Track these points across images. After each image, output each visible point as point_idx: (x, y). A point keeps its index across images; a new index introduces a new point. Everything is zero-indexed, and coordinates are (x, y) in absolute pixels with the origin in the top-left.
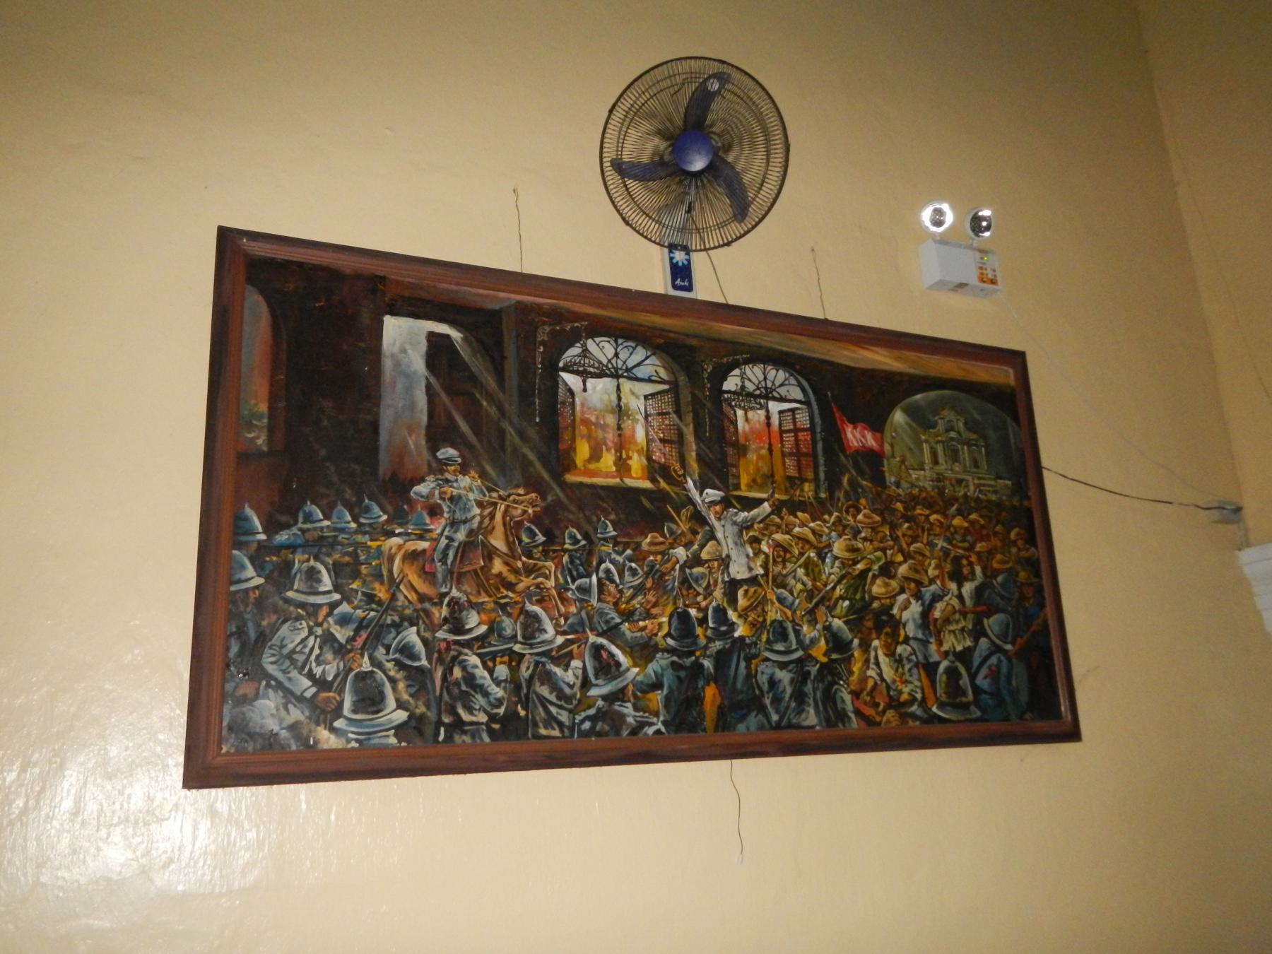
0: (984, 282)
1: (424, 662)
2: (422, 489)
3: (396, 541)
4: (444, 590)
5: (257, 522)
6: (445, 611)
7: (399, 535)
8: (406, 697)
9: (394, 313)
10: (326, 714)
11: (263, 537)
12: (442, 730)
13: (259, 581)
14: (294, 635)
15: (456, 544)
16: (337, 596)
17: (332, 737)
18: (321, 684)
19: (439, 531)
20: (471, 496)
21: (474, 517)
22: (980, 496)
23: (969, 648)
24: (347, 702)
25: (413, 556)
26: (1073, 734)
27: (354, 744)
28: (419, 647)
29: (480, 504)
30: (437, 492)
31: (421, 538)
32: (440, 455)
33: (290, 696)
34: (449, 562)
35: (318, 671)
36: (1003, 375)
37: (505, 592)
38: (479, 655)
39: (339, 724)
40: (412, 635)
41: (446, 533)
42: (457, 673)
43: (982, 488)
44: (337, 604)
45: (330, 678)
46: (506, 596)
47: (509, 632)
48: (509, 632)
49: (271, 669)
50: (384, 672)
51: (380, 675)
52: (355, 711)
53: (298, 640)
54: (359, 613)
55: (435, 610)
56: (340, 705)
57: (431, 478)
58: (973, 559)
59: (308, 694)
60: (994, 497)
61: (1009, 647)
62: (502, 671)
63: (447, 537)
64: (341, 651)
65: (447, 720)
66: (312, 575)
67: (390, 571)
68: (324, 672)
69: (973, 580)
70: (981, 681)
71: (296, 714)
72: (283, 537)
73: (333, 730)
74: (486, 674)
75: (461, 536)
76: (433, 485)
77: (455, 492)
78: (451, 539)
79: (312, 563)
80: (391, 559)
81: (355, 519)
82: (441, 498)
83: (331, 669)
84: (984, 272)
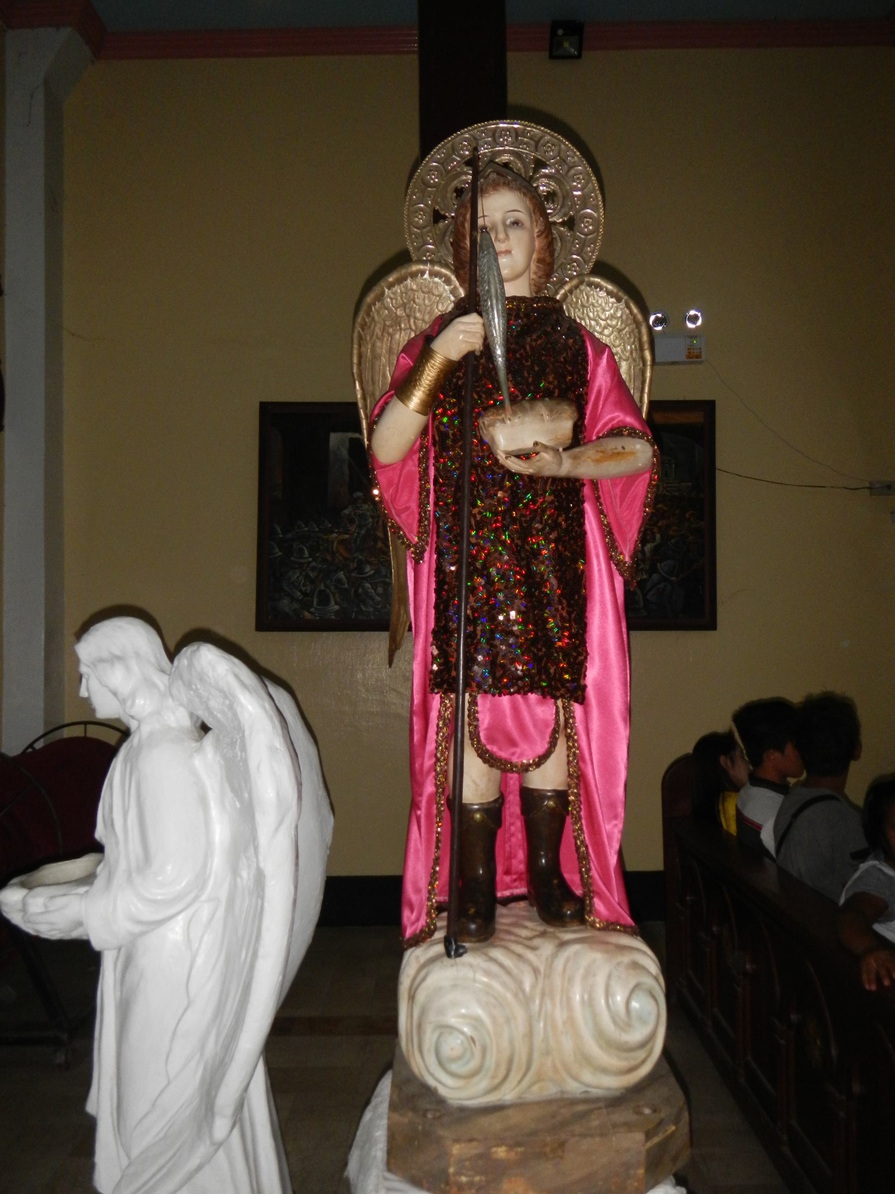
0: (691, 358)
1: (346, 586)
2: (346, 512)
3: (335, 535)
4: (355, 555)
5: (279, 529)
6: (355, 565)
7: (336, 533)
8: (338, 600)
9: (335, 431)
10: (307, 606)
11: (281, 536)
12: (354, 614)
13: (280, 554)
14: (295, 575)
15: (361, 535)
16: (311, 559)
17: (309, 615)
18: (305, 594)
19: (354, 530)
20: (368, 514)
21: (369, 523)
22: (667, 493)
23: (645, 579)
24: (315, 603)
25: (342, 542)
26: (712, 625)
27: (318, 618)
28: (344, 579)
29: (372, 517)
30: (353, 513)
31: (345, 533)
32: (355, 495)
33: (293, 599)
34: (358, 543)
35: (304, 589)
36: (696, 418)
37: (383, 556)
38: (370, 583)
39: (312, 610)
40: (341, 575)
41: (357, 531)
42: (360, 590)
43: (668, 489)
44: (312, 562)
45: (308, 592)
46: (383, 558)
47: (384, 573)
48: (384, 573)
49: (285, 588)
50: (330, 590)
51: (328, 591)
52: (318, 604)
53: (296, 577)
54: (320, 566)
55: (351, 565)
56: (312, 602)
57: (350, 506)
58: (655, 530)
59: (300, 598)
60: (677, 494)
61: (673, 579)
62: (380, 590)
63: (357, 533)
64: (312, 582)
65: (355, 610)
66: (301, 551)
67: (332, 548)
68: (306, 590)
69: (653, 542)
70: (648, 597)
71: (296, 606)
72: (289, 536)
73: (309, 612)
74: (373, 591)
75: (363, 532)
76: (351, 510)
77: (361, 512)
78: (359, 533)
79: (301, 546)
80: (333, 543)
81: (317, 527)
82: (355, 516)
83: (308, 589)
84: (692, 351)
